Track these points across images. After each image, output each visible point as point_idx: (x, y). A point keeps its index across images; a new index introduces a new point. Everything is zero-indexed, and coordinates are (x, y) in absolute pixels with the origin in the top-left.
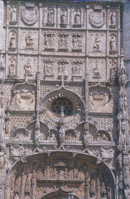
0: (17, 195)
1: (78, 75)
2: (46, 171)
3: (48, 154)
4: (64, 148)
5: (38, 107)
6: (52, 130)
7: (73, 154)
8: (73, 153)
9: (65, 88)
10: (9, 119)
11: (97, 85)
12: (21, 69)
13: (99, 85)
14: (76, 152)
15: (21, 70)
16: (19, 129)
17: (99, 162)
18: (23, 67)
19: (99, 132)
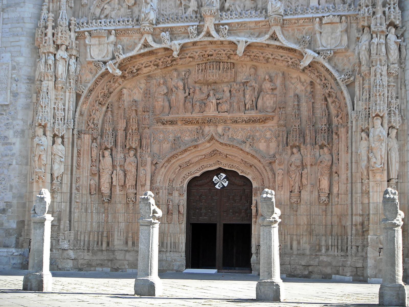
0: (107, 153)
2: (176, 94)
3: (173, 51)
4: (213, 33)
8: (239, 42)
14: (244, 39)
17: (306, 62)
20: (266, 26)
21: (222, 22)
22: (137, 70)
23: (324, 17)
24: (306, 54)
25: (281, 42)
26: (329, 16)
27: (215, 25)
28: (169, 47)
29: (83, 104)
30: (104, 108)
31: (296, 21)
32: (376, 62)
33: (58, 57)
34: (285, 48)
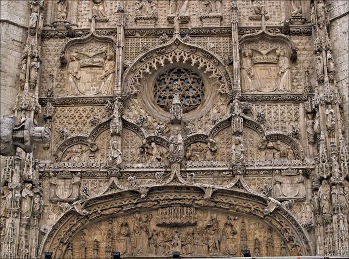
1: (216, 14)
4: (181, 179)
5: (117, 87)
6: (153, 139)
7: (206, 191)
8: (206, 188)
9: (183, 42)
10: (50, 118)
11: (260, 32)
12: (83, 9)
13: (263, 33)
14: (211, 186)
15: (83, 12)
16: (72, 139)
18: (87, 5)
19: (270, 138)
20: (230, 175)
21: (187, 169)
22: (102, 211)
23: (283, 170)
24: (270, 201)
25: (246, 190)
26: (287, 169)
27: (181, 171)
28: (138, 190)
29: (47, 242)
30: (65, 247)
31: (257, 172)
32: (338, 209)
33: (24, 194)
34: (250, 195)
